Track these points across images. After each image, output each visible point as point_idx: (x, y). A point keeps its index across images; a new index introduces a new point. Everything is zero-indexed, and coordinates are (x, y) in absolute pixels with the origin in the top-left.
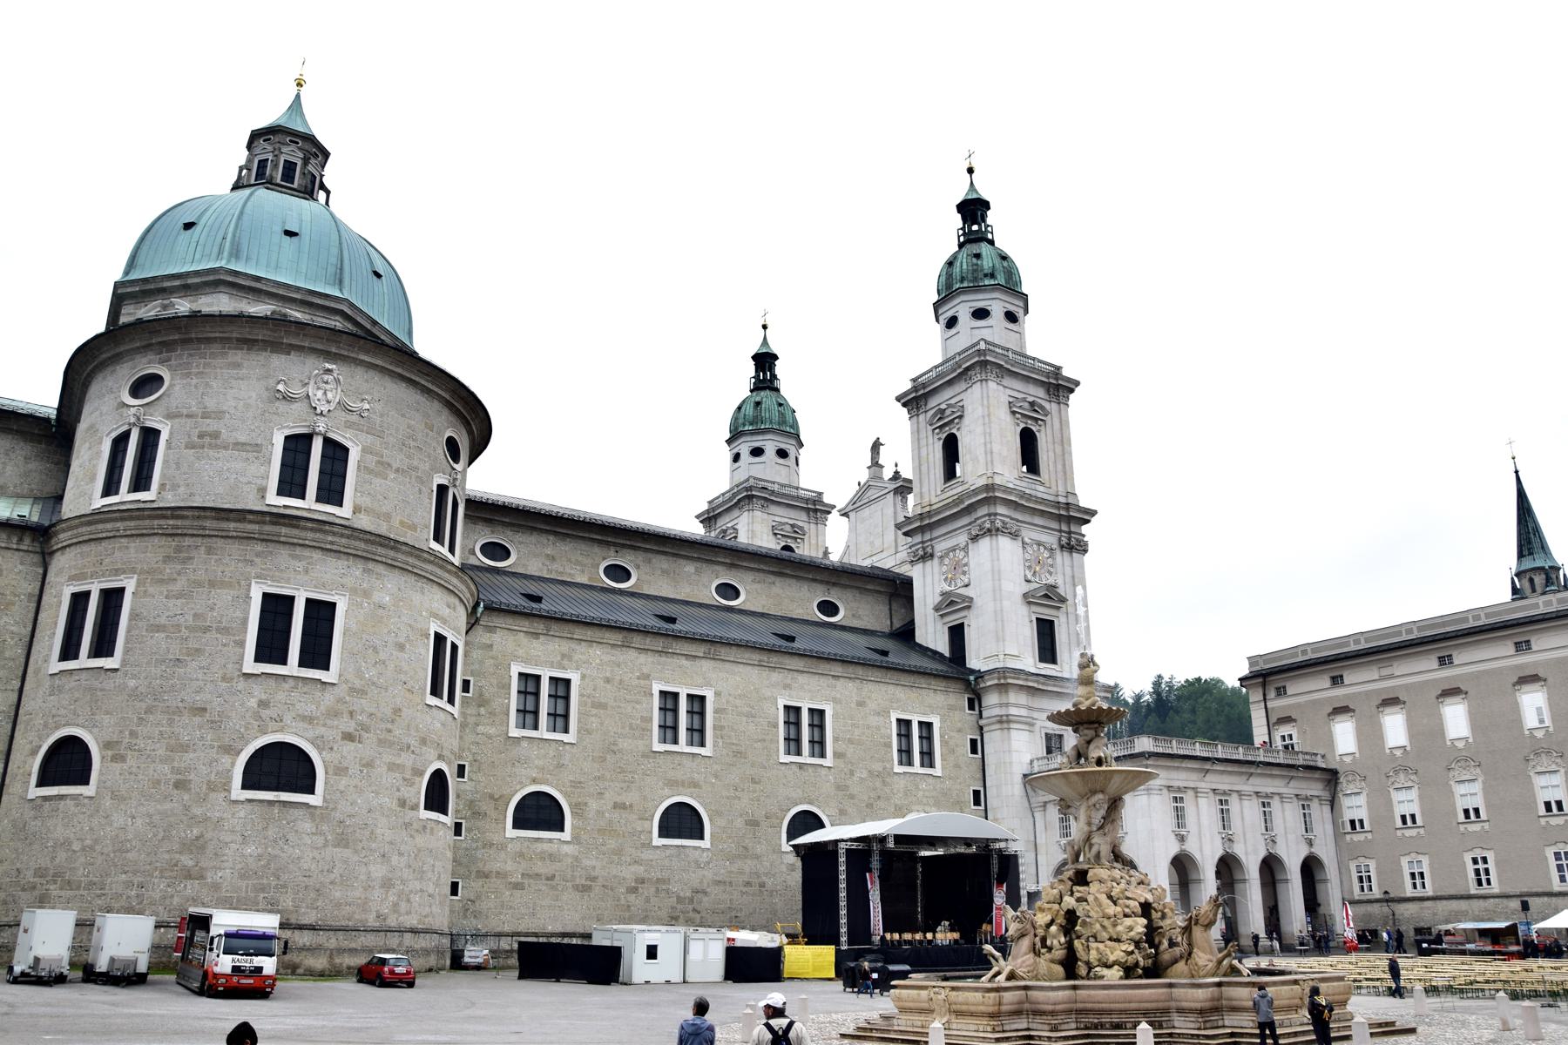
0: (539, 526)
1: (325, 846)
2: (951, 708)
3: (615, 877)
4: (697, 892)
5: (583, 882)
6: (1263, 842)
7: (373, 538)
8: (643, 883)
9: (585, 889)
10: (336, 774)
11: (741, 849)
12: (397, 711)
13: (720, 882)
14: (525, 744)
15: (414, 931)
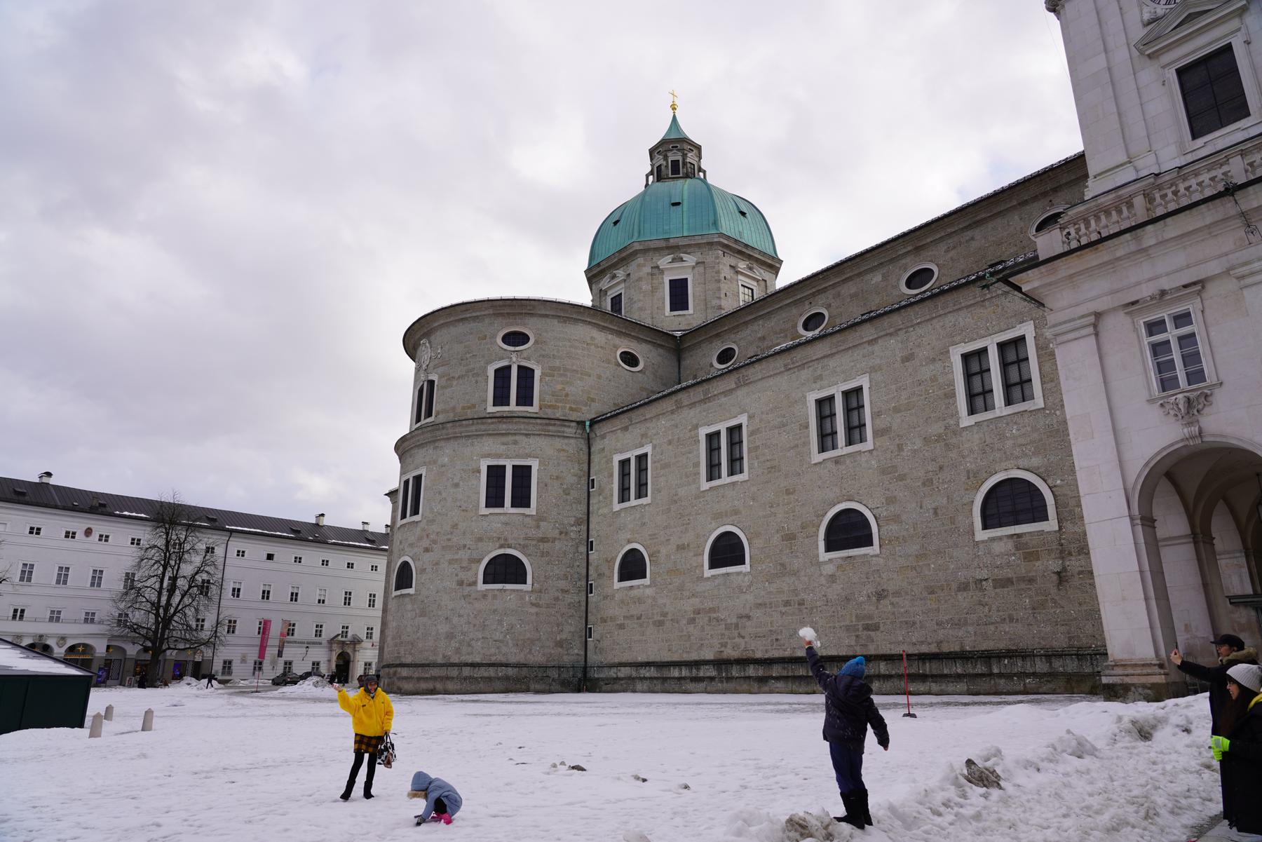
0: (747, 319)
3: (680, 611)
4: (741, 617)
5: (659, 618)
8: (699, 613)
9: (660, 624)
10: (420, 574)
12: (455, 526)
13: (760, 604)
14: (623, 515)
15: (473, 665)
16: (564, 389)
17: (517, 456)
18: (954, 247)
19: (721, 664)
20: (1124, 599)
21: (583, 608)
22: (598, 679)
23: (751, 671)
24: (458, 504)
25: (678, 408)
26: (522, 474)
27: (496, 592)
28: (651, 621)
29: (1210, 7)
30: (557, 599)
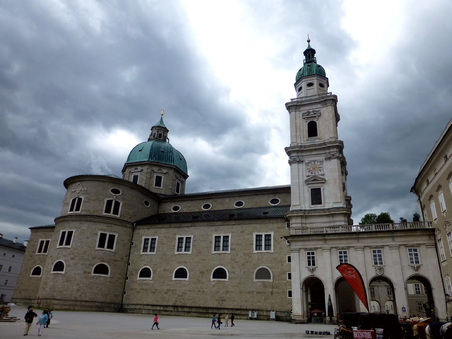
1: (64, 282)
2: (279, 228)
6: (374, 270)
7: (81, 216)
8: (169, 291)
10: (68, 267)
11: (198, 280)
13: (191, 290)
15: (86, 301)
16: (128, 211)
17: (111, 231)
18: (250, 199)
19: (174, 306)
20: (298, 303)
21: (124, 284)
22: (127, 308)
23: (185, 310)
24: (88, 244)
25: (170, 227)
26: (112, 238)
27: (97, 277)
28: (151, 292)
29: (318, 179)
30: (117, 281)
